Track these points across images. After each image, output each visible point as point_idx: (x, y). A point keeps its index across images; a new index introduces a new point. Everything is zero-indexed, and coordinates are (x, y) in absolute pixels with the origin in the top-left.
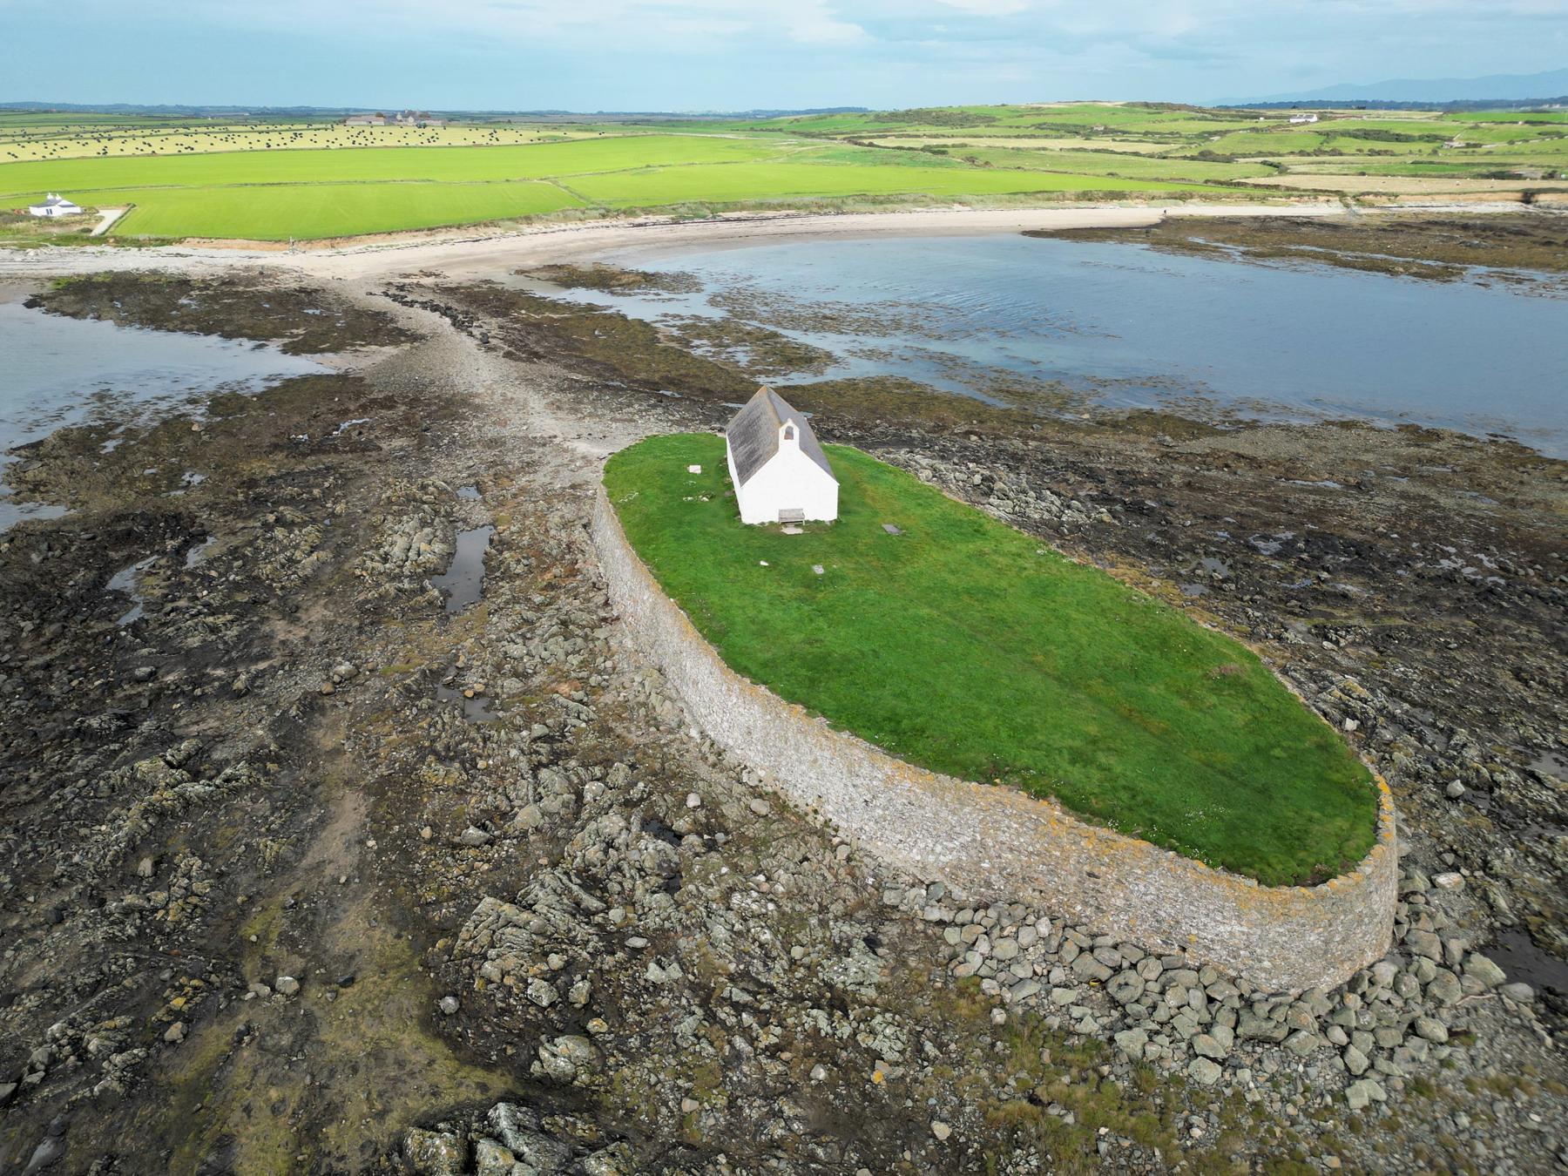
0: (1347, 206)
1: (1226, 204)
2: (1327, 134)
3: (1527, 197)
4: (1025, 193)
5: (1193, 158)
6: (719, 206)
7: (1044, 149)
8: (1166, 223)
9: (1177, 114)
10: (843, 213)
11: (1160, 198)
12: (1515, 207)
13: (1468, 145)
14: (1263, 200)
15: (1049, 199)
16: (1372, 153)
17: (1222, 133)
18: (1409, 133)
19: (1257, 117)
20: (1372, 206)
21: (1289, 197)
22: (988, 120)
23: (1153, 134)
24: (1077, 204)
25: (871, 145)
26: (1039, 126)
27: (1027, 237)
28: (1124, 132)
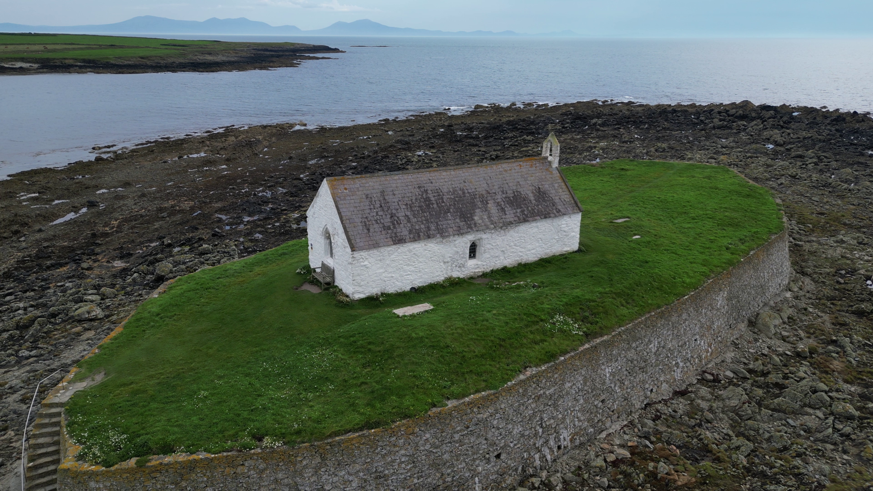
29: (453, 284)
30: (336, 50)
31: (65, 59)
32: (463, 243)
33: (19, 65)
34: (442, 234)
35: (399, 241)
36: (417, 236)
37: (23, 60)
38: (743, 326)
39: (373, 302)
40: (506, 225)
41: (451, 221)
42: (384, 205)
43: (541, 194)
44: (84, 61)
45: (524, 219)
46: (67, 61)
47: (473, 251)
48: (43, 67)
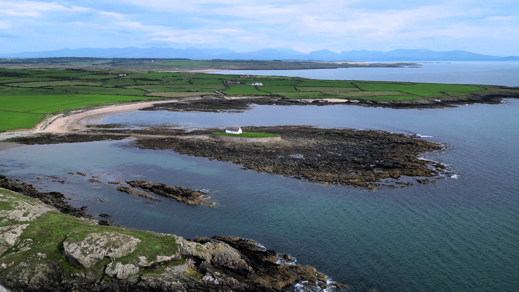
0: (178, 100)
1: (159, 101)
2: (134, 79)
3: (202, 96)
4: (121, 101)
5: (114, 87)
6: (68, 110)
7: (69, 85)
8: (156, 105)
9: (85, 73)
10: (93, 109)
11: (146, 101)
12: (200, 98)
13: (166, 82)
14: (164, 100)
15: (127, 102)
16: (151, 84)
17: (108, 79)
18: (153, 79)
19: (109, 74)
20: (182, 100)
21: (168, 99)
22: (27, 75)
23: (89, 79)
24: (132, 103)
25: (18, 87)
26: (50, 77)
27: (141, 111)
28: (80, 79)
31: (367, 100)
32: (231, 131)
36: (229, 130)
37: (358, 100)
40: (233, 131)
44: (372, 101)
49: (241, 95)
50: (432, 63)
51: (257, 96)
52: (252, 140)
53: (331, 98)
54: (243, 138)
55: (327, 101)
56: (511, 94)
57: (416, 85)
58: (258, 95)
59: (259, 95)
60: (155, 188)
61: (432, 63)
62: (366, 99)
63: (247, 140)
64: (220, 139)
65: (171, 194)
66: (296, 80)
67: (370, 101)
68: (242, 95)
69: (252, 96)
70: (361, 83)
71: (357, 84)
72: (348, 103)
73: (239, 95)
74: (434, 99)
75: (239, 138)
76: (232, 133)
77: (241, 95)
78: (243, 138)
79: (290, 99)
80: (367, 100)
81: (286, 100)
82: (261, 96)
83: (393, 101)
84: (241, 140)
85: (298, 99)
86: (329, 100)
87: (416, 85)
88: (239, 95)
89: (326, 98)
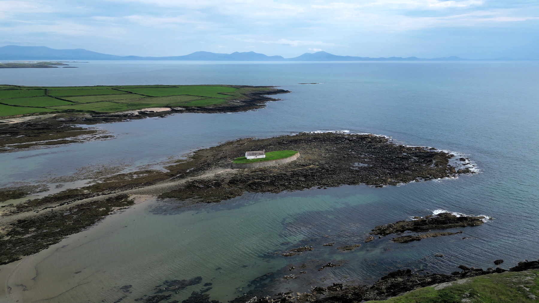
29: (254, 159)
30: (287, 92)
31: (192, 106)
32: (255, 156)
33: (179, 109)
34: (254, 156)
35: (250, 156)
36: (252, 155)
37: (180, 107)
38: (277, 164)
39: (248, 159)
40: (259, 155)
41: (254, 155)
42: (250, 153)
43: (262, 153)
45: (260, 155)
46: (193, 107)
47: (256, 157)
48: (187, 110)
49: (20, 116)
50: (68, 62)
51: (45, 114)
52: (287, 161)
53: (150, 108)
54: (279, 161)
55: (153, 111)
56: (260, 91)
57: (178, 87)
58: (46, 112)
59: (46, 113)
60: (424, 225)
61: (68, 62)
62: (192, 106)
63: (282, 162)
64: (252, 168)
65: (447, 223)
66: (35, 89)
67: (195, 107)
68: (22, 115)
69: (36, 115)
70: (123, 88)
71: (130, 90)
72: (174, 111)
73: (18, 116)
74: (233, 100)
75: (274, 161)
76: (256, 158)
77: (20, 116)
78: (278, 161)
79: (110, 113)
80: (192, 106)
81: (101, 115)
82: (50, 113)
83: (214, 105)
84: (276, 163)
85: (118, 112)
86: (156, 110)
87: (178, 87)
88: (18, 116)
89: (144, 108)
